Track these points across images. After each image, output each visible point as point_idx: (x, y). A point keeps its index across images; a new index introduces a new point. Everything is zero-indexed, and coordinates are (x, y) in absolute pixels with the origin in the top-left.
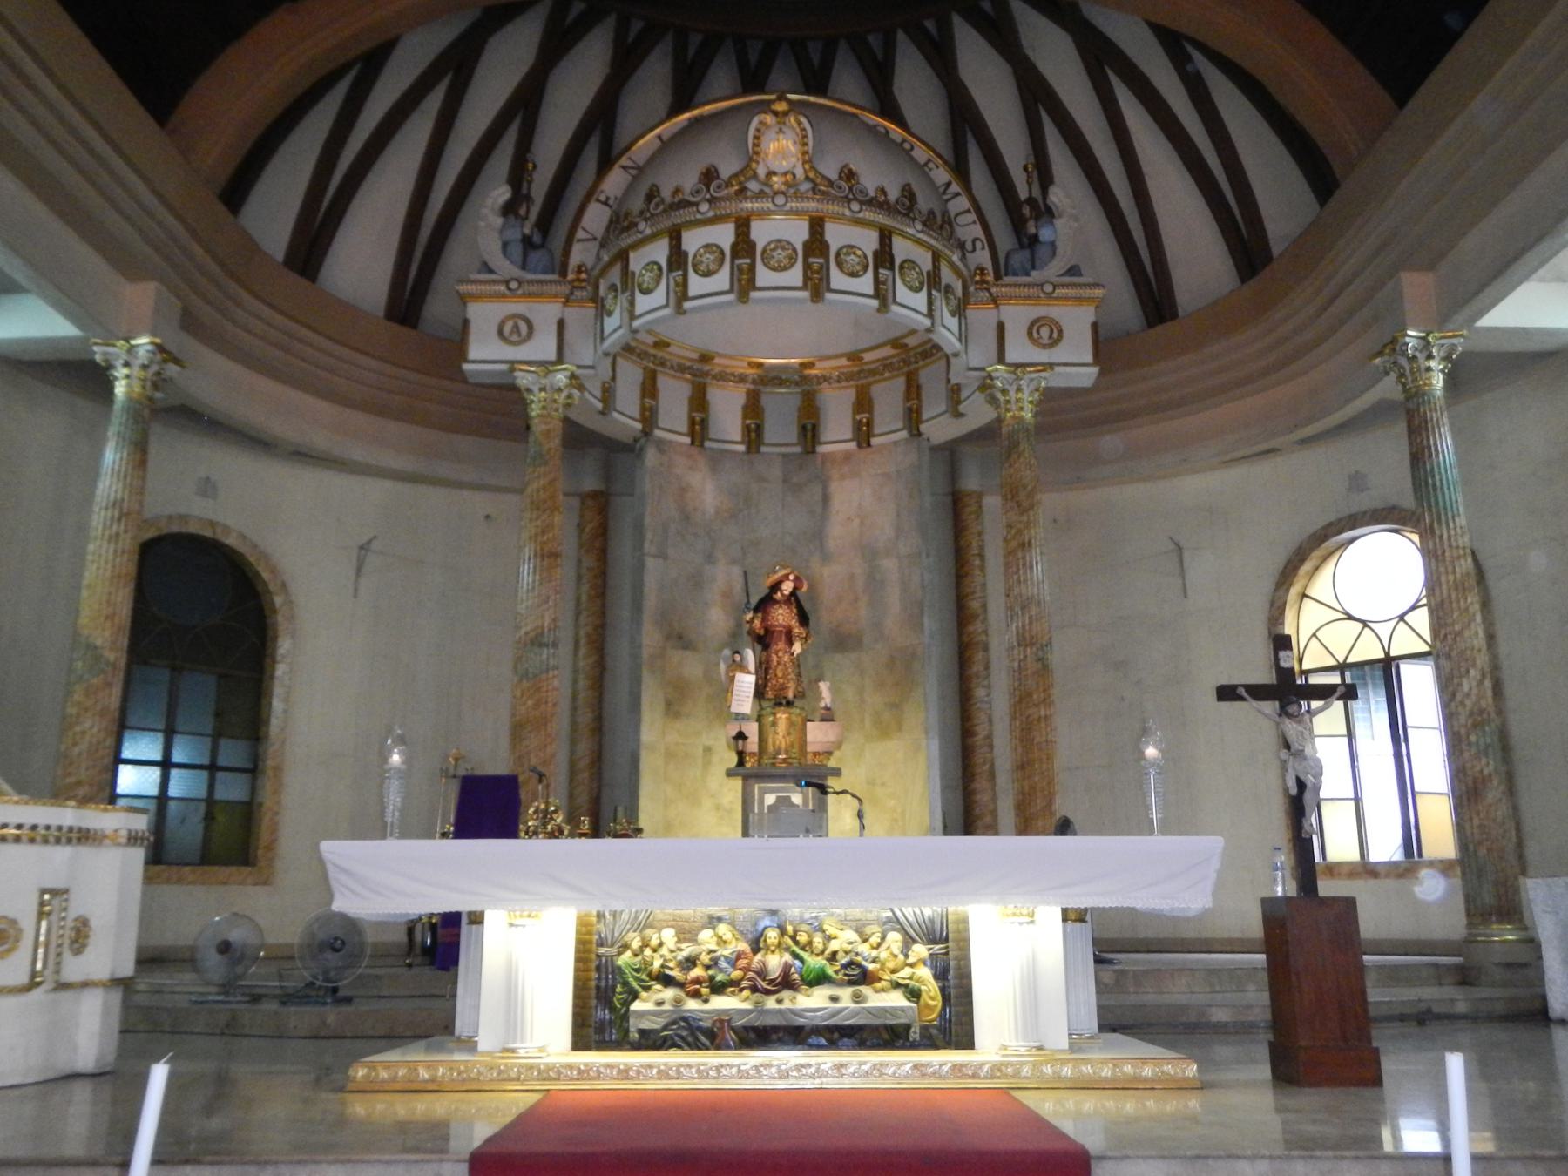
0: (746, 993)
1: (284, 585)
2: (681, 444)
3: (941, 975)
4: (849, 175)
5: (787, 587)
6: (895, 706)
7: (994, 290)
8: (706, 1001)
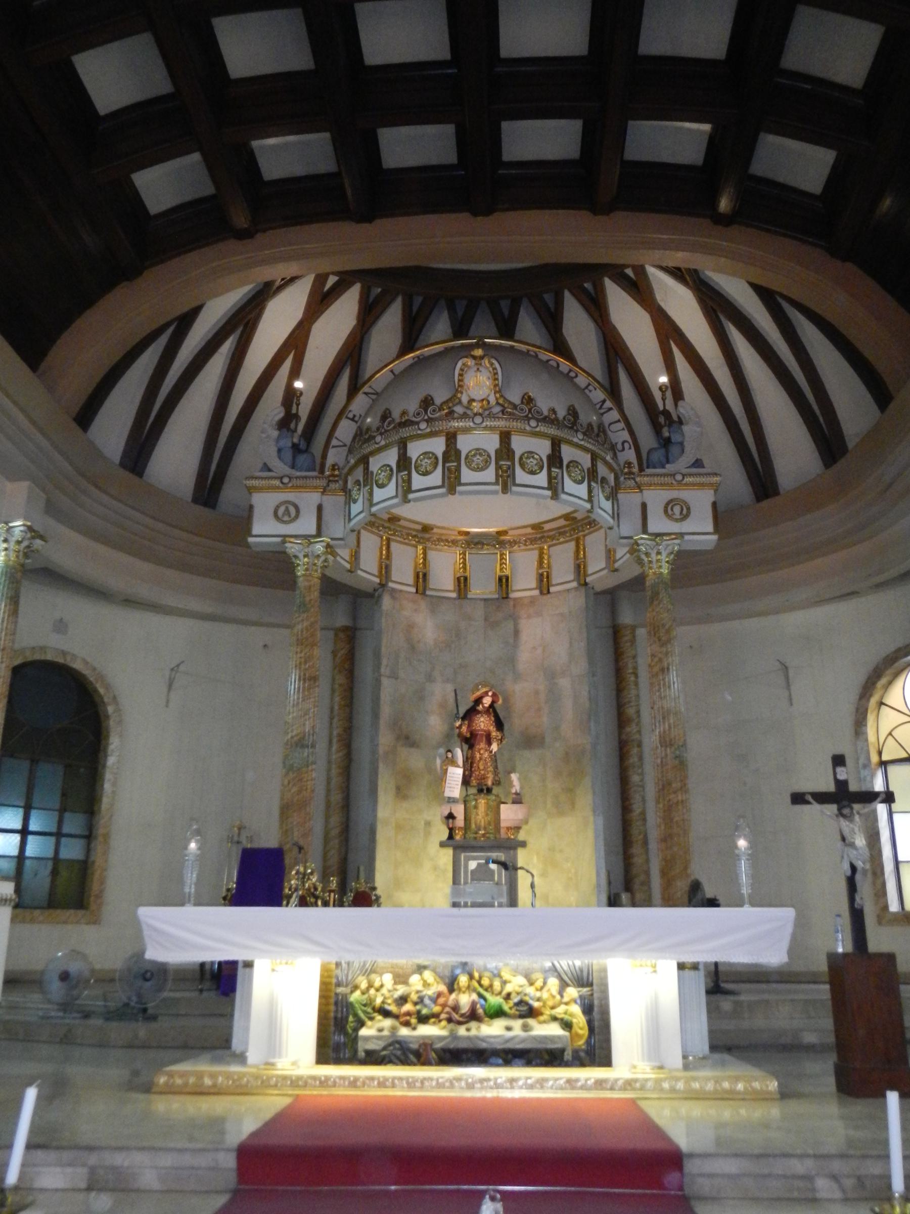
0: (444, 1023)
1: (115, 698)
2: (409, 592)
3: (588, 1010)
4: (528, 400)
5: (487, 701)
6: (570, 791)
7: (638, 479)
8: (414, 1029)
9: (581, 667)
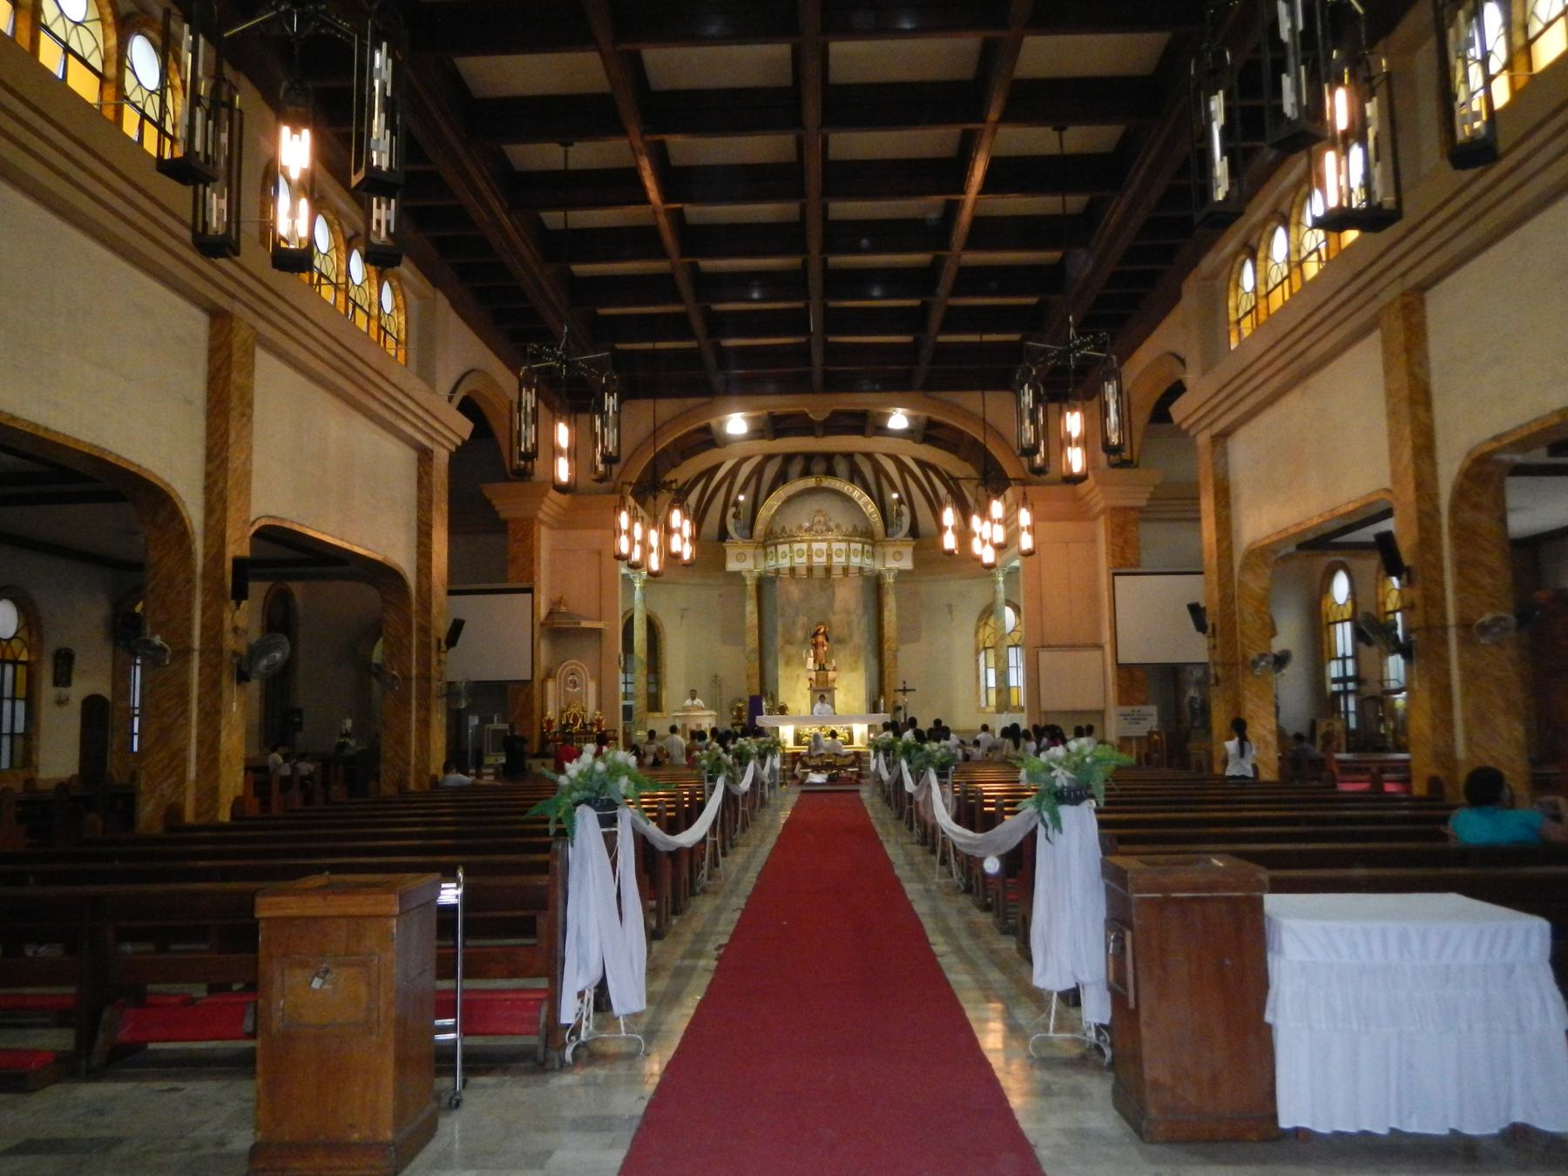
6: (856, 662)
9: (860, 611)
